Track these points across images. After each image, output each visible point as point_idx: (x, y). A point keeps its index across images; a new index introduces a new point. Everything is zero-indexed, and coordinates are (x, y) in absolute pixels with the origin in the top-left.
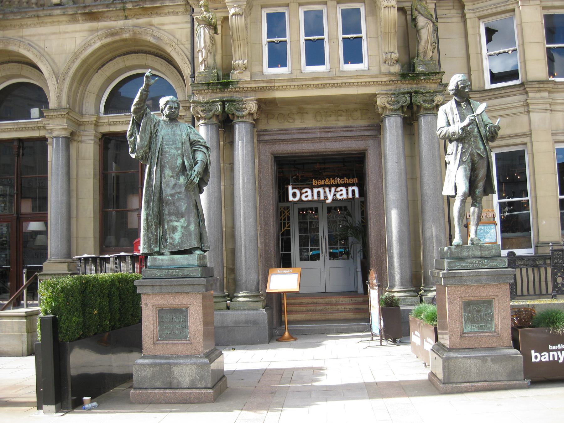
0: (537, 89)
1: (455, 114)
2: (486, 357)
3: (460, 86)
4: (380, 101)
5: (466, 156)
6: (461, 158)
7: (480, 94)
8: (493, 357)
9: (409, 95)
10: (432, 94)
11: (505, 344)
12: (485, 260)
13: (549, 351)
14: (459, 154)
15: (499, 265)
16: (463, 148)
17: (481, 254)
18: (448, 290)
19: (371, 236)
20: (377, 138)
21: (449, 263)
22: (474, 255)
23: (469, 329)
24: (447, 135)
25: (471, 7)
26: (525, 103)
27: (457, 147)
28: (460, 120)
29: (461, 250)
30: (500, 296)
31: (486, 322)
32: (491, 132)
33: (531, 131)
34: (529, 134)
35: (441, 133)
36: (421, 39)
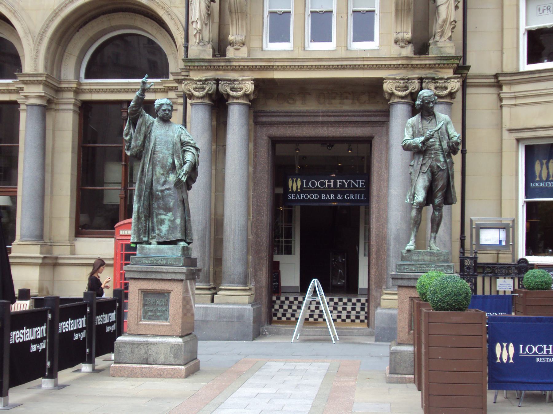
4: (387, 87)
9: (420, 81)
10: (446, 81)
15: (446, 270)
19: (372, 232)
20: (385, 125)
36: (439, 17)
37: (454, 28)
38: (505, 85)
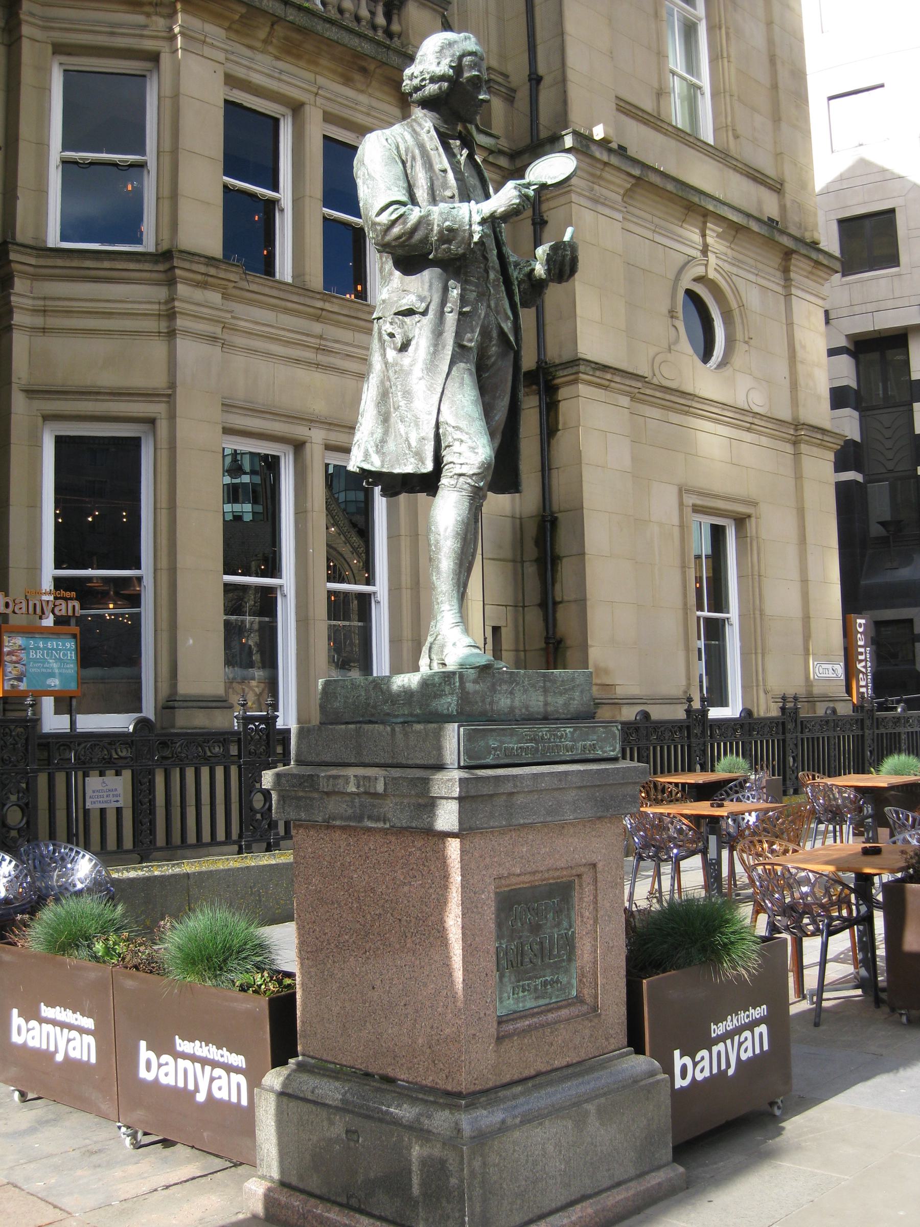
0: (199, 277)
1: (437, 167)
2: (585, 1106)
3: (467, 75)
5: (473, 332)
6: (458, 335)
8: (603, 1100)
11: (612, 1040)
12: (568, 730)
13: (708, 1044)
14: (451, 319)
15: (601, 748)
16: (463, 299)
17: (546, 704)
18: (463, 851)
21: (471, 737)
22: (527, 707)
23: (511, 1001)
24: (418, 236)
26: (163, 307)
27: (445, 290)
28: (460, 194)
29: (493, 689)
31: (556, 967)
32: (562, 264)
33: (172, 385)
34: (168, 396)
35: (394, 223)
38: (20, 277)
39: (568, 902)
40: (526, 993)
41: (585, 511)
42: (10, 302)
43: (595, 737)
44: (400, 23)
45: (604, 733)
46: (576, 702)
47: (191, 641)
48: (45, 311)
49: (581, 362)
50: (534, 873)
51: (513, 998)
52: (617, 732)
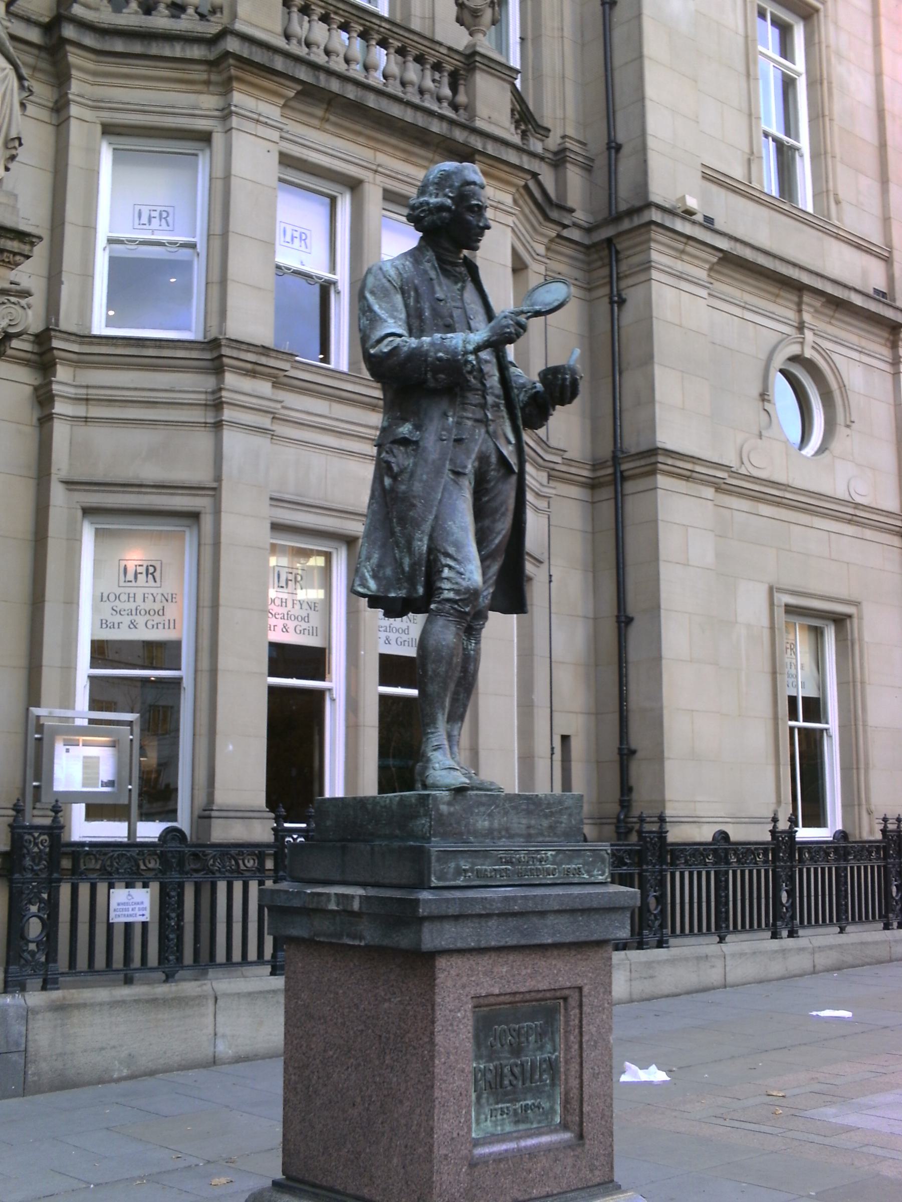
0: (249, 366)
7: (81, 343)
12: (550, 853)
15: (588, 872)
23: (489, 1123)
25: (87, 89)
26: (210, 397)
30: (586, 990)
33: (218, 478)
34: (214, 491)
37: (13, 158)
38: (61, 364)
39: (552, 1025)
40: (505, 1116)
41: (662, 611)
42: (51, 390)
43: (581, 861)
44: (467, 93)
45: (591, 856)
46: (563, 825)
47: (231, 747)
48: (87, 400)
49: (660, 452)
50: (515, 993)
51: (491, 1121)
52: (606, 856)
